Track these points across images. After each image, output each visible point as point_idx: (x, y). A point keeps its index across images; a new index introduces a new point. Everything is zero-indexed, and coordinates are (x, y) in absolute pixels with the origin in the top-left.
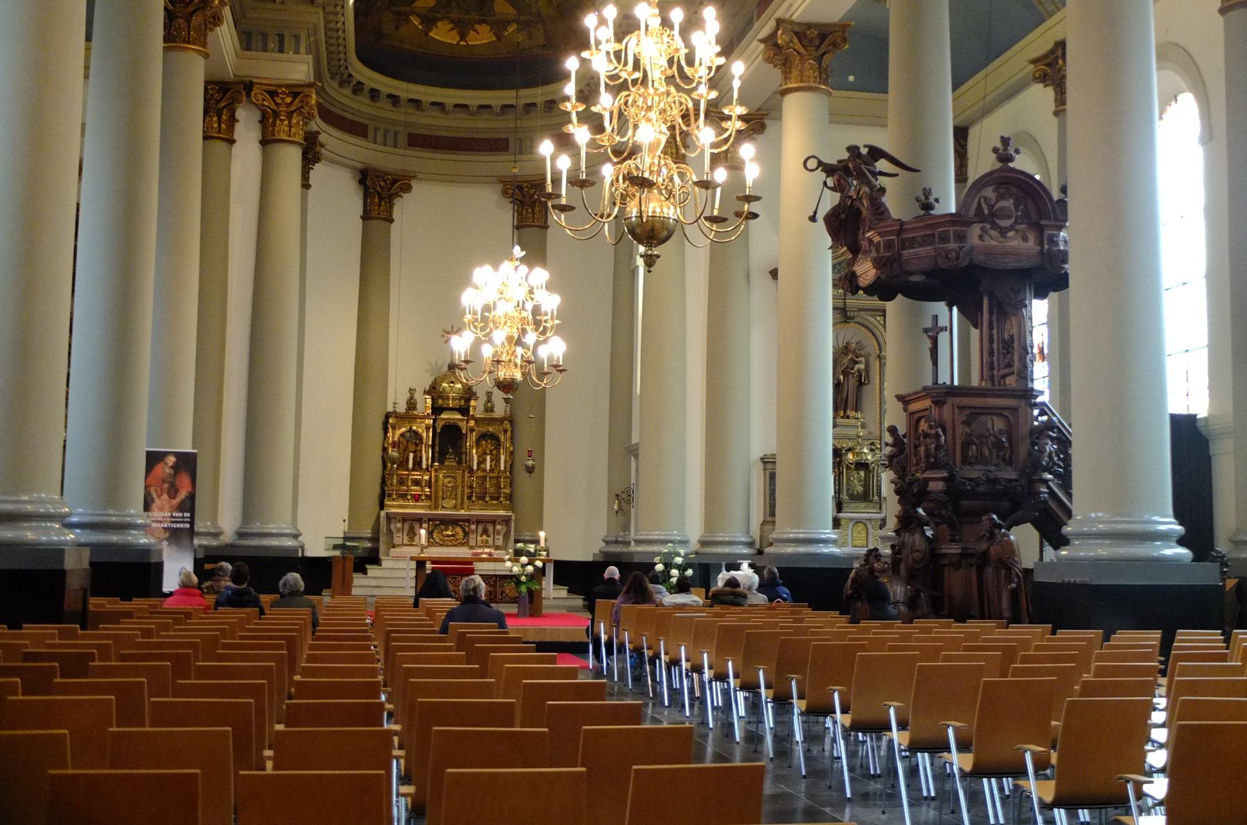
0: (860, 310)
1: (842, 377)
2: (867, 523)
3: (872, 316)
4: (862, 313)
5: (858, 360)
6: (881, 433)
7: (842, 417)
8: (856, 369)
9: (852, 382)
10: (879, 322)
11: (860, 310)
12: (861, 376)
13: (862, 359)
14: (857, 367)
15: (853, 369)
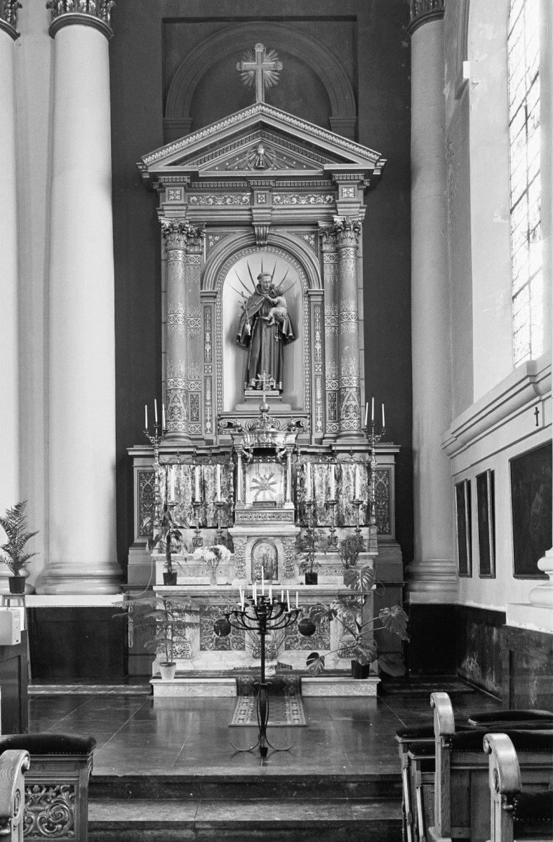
0: (275, 225)
1: (248, 327)
2: (277, 541)
3: (297, 234)
4: (282, 231)
5: (275, 300)
6: (311, 409)
7: (255, 388)
8: (271, 314)
9: (268, 337)
10: (307, 242)
11: (275, 225)
12: (282, 324)
13: (282, 299)
14: (273, 310)
15: (267, 315)
